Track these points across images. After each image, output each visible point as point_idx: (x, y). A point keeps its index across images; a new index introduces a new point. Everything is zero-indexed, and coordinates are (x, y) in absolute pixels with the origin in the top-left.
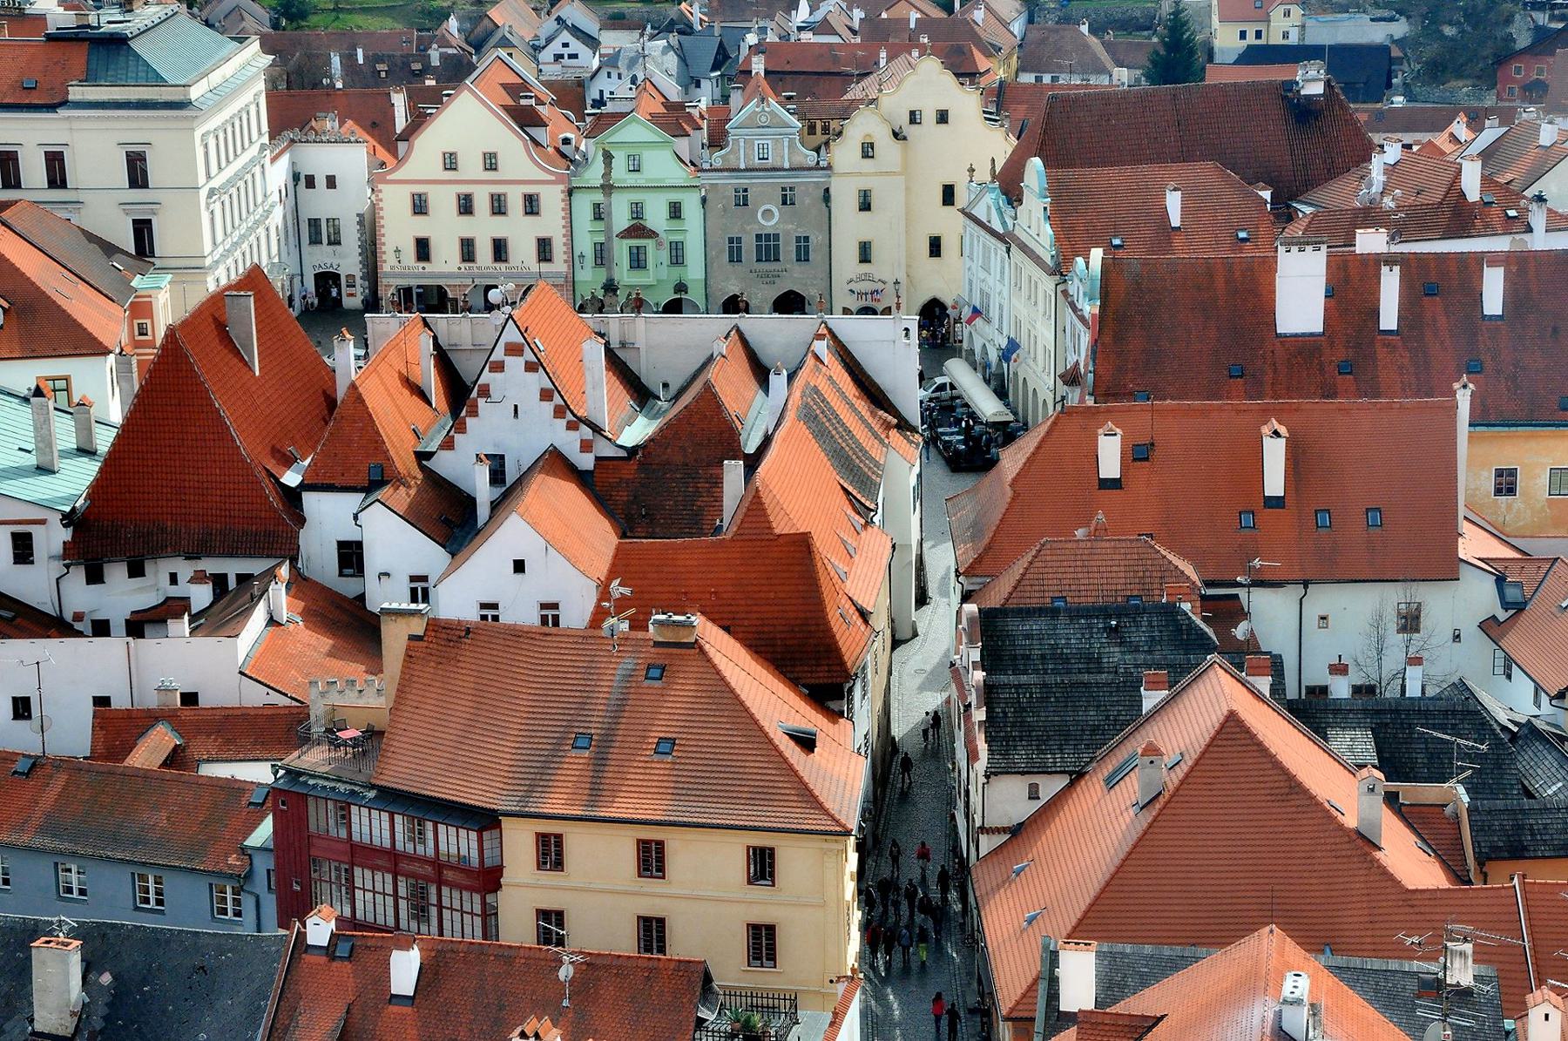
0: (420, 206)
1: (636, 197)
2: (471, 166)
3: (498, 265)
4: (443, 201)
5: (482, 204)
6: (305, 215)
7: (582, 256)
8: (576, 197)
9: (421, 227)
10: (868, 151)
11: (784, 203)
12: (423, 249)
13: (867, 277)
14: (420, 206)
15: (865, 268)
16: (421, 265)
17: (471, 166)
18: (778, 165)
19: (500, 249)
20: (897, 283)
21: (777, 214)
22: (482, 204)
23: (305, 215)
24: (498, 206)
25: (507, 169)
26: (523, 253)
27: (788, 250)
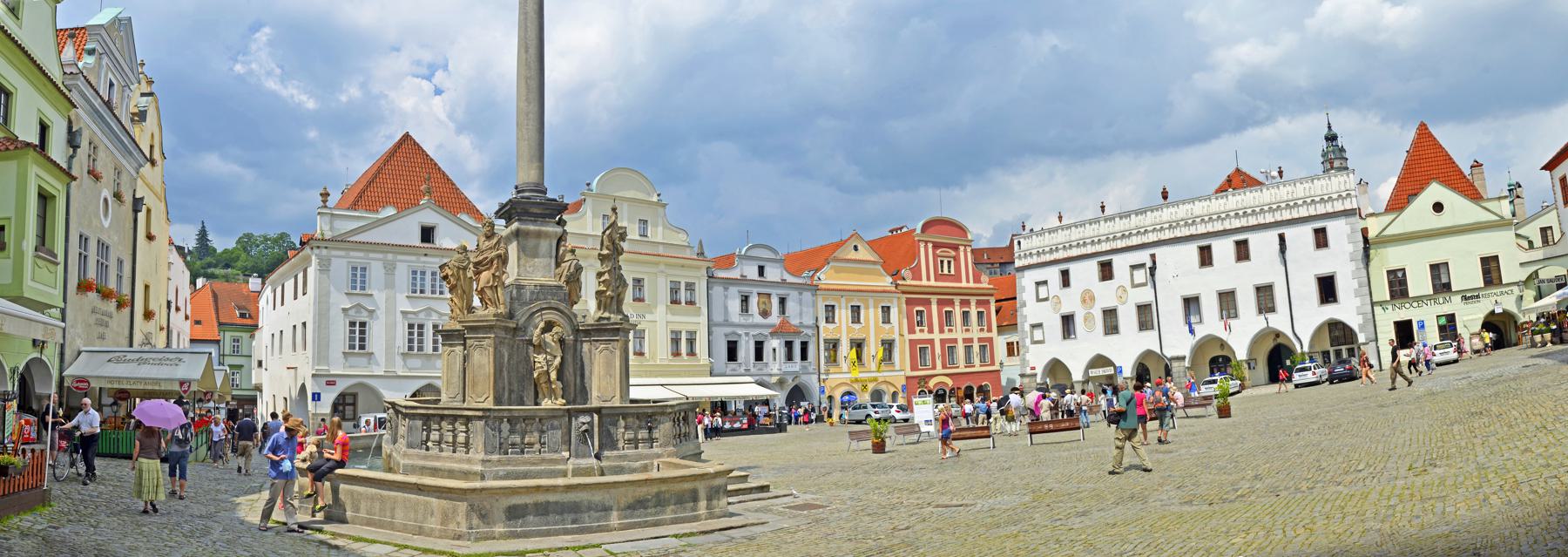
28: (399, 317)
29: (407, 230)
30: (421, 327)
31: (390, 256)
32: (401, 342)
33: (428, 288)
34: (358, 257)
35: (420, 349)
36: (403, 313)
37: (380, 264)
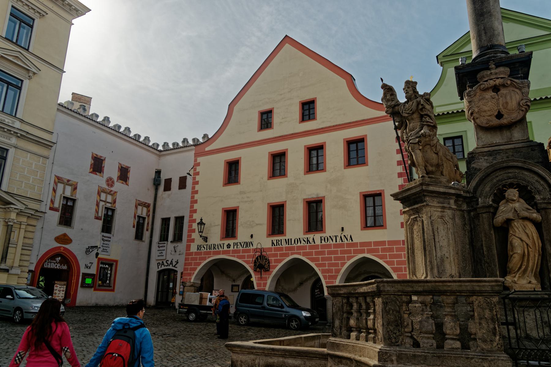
0: (233, 171)
2: (287, 120)
3: (310, 236)
4: (255, 163)
5: (296, 161)
6: (160, 215)
9: (231, 196)
14: (233, 171)
16: (226, 242)
17: (287, 120)
22: (296, 161)
23: (160, 215)
24: (315, 157)
25: (324, 116)
26: (343, 219)
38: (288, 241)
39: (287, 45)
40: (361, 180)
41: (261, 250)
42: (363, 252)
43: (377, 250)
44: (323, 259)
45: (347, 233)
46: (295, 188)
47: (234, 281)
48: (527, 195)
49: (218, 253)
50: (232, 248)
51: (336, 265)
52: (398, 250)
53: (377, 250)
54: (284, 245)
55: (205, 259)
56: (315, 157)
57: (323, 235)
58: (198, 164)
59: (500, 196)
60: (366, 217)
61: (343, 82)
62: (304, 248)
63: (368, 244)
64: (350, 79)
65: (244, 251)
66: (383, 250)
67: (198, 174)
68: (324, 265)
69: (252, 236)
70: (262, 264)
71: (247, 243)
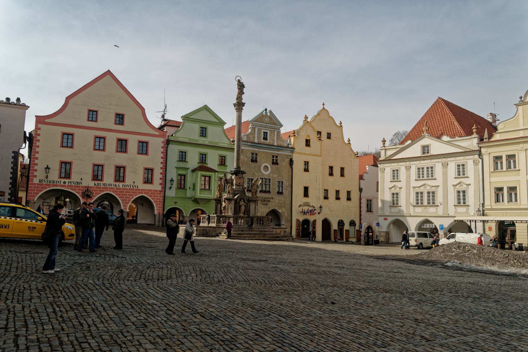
0: (67, 140)
1: (204, 150)
2: (106, 120)
3: (117, 184)
7: (172, 180)
8: (171, 146)
9: (67, 155)
10: (308, 143)
11: (273, 163)
12: (66, 169)
13: (307, 204)
14: (67, 140)
15: (306, 200)
17: (106, 120)
18: (271, 143)
19: (120, 172)
20: (321, 207)
21: (270, 169)
24: (122, 145)
25: (128, 126)
26: (134, 178)
27: (274, 188)
28: (412, 189)
29: (415, 150)
30: (422, 193)
31: (408, 163)
32: (413, 200)
33: (425, 175)
34: (395, 166)
35: (422, 203)
36: (414, 187)
37: (404, 167)
38: (104, 184)
39: (108, 76)
40: (144, 161)
41: (88, 187)
42: (142, 193)
43: (148, 193)
44: (123, 195)
45: (136, 184)
46: (111, 158)
47: (45, 200)
48: (244, 201)
49: (57, 186)
50: (67, 184)
51: (129, 198)
52: (157, 194)
53: (148, 193)
54: (102, 186)
55: (46, 188)
56: (122, 145)
57: (124, 184)
58: (40, 129)
59: (240, 200)
60: (124, 172)
61: (140, 111)
62: (113, 188)
63: (145, 190)
64: (143, 109)
65: (75, 187)
66: (151, 193)
67: (39, 135)
68: (123, 197)
69: (81, 179)
70: (87, 194)
71: (78, 183)
